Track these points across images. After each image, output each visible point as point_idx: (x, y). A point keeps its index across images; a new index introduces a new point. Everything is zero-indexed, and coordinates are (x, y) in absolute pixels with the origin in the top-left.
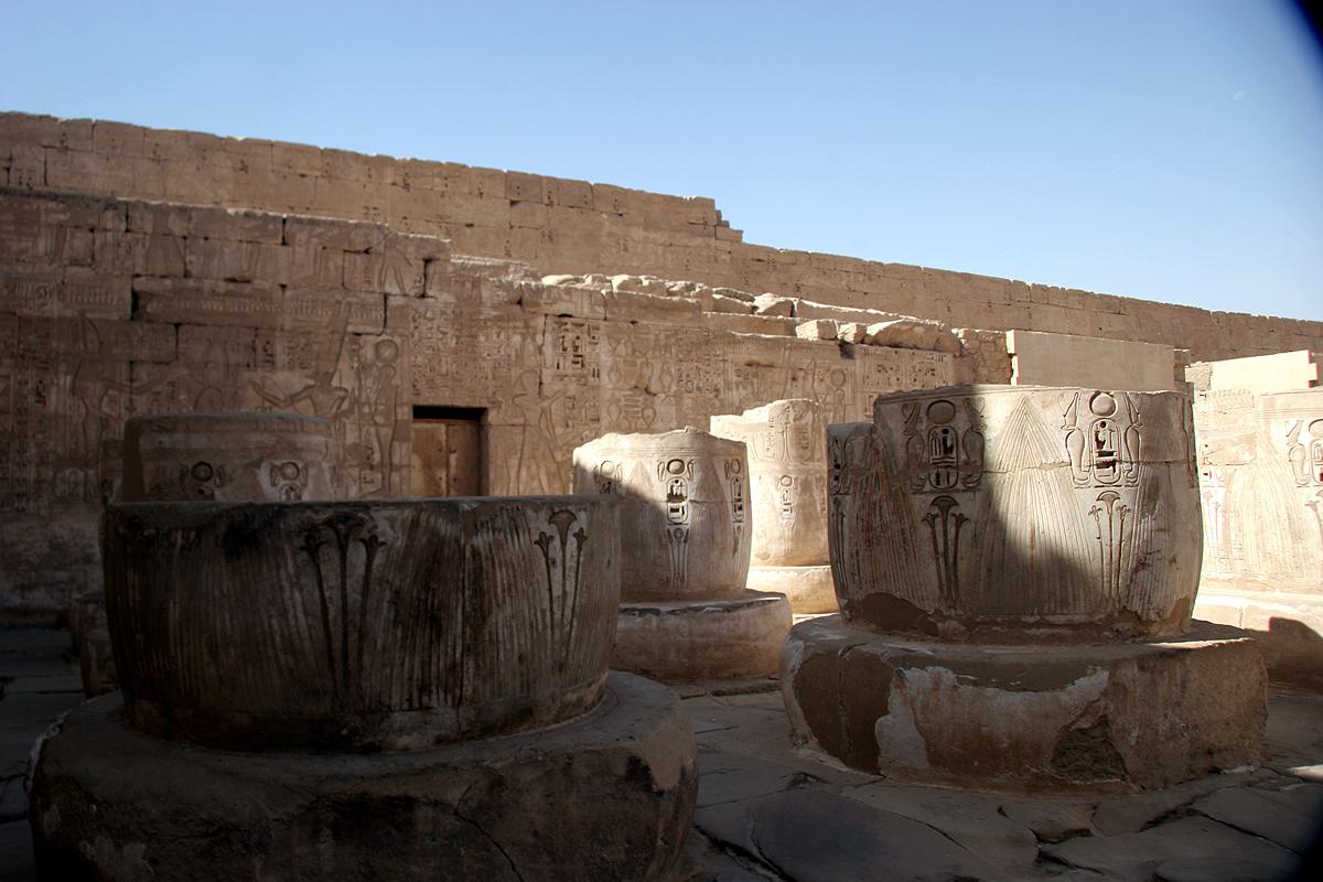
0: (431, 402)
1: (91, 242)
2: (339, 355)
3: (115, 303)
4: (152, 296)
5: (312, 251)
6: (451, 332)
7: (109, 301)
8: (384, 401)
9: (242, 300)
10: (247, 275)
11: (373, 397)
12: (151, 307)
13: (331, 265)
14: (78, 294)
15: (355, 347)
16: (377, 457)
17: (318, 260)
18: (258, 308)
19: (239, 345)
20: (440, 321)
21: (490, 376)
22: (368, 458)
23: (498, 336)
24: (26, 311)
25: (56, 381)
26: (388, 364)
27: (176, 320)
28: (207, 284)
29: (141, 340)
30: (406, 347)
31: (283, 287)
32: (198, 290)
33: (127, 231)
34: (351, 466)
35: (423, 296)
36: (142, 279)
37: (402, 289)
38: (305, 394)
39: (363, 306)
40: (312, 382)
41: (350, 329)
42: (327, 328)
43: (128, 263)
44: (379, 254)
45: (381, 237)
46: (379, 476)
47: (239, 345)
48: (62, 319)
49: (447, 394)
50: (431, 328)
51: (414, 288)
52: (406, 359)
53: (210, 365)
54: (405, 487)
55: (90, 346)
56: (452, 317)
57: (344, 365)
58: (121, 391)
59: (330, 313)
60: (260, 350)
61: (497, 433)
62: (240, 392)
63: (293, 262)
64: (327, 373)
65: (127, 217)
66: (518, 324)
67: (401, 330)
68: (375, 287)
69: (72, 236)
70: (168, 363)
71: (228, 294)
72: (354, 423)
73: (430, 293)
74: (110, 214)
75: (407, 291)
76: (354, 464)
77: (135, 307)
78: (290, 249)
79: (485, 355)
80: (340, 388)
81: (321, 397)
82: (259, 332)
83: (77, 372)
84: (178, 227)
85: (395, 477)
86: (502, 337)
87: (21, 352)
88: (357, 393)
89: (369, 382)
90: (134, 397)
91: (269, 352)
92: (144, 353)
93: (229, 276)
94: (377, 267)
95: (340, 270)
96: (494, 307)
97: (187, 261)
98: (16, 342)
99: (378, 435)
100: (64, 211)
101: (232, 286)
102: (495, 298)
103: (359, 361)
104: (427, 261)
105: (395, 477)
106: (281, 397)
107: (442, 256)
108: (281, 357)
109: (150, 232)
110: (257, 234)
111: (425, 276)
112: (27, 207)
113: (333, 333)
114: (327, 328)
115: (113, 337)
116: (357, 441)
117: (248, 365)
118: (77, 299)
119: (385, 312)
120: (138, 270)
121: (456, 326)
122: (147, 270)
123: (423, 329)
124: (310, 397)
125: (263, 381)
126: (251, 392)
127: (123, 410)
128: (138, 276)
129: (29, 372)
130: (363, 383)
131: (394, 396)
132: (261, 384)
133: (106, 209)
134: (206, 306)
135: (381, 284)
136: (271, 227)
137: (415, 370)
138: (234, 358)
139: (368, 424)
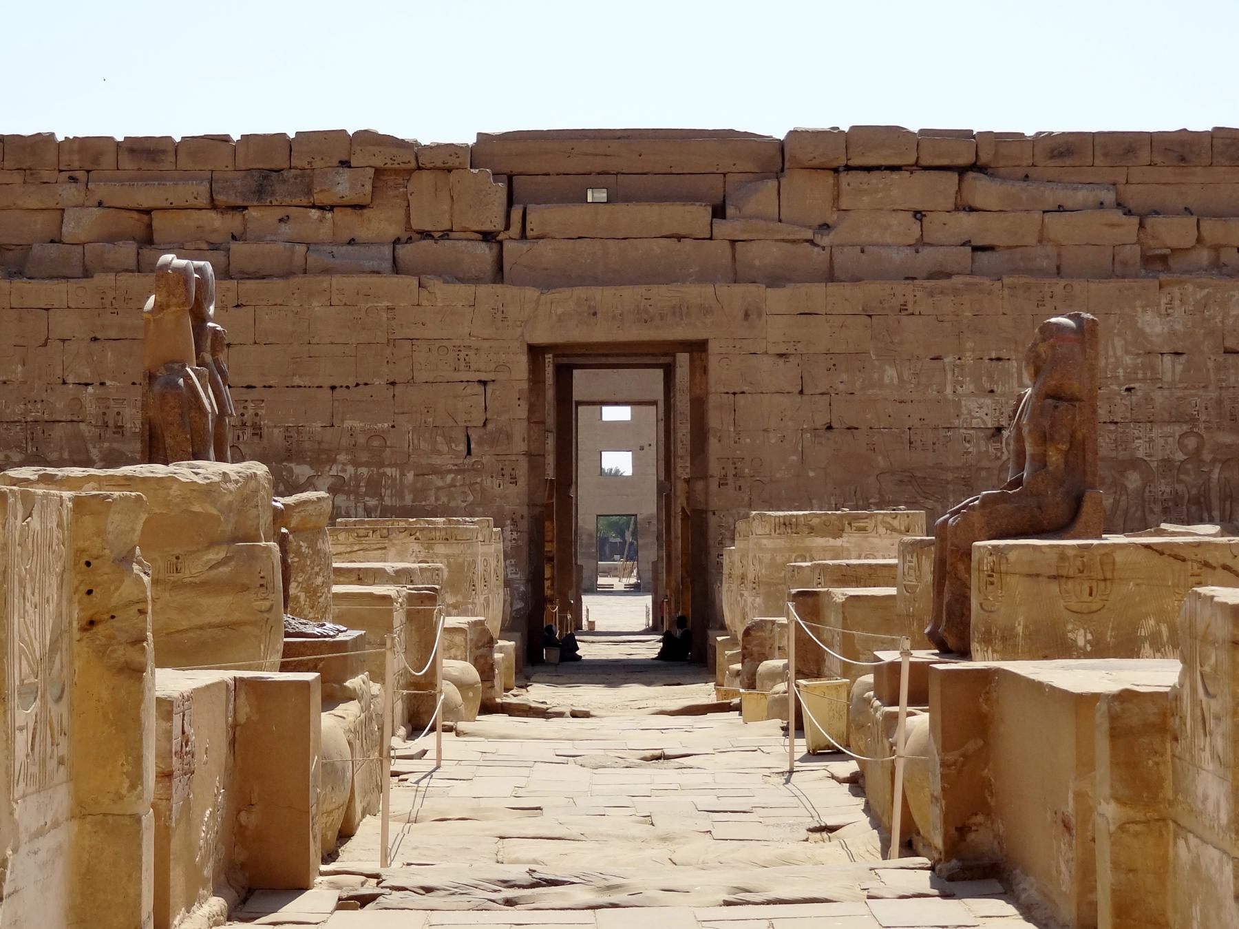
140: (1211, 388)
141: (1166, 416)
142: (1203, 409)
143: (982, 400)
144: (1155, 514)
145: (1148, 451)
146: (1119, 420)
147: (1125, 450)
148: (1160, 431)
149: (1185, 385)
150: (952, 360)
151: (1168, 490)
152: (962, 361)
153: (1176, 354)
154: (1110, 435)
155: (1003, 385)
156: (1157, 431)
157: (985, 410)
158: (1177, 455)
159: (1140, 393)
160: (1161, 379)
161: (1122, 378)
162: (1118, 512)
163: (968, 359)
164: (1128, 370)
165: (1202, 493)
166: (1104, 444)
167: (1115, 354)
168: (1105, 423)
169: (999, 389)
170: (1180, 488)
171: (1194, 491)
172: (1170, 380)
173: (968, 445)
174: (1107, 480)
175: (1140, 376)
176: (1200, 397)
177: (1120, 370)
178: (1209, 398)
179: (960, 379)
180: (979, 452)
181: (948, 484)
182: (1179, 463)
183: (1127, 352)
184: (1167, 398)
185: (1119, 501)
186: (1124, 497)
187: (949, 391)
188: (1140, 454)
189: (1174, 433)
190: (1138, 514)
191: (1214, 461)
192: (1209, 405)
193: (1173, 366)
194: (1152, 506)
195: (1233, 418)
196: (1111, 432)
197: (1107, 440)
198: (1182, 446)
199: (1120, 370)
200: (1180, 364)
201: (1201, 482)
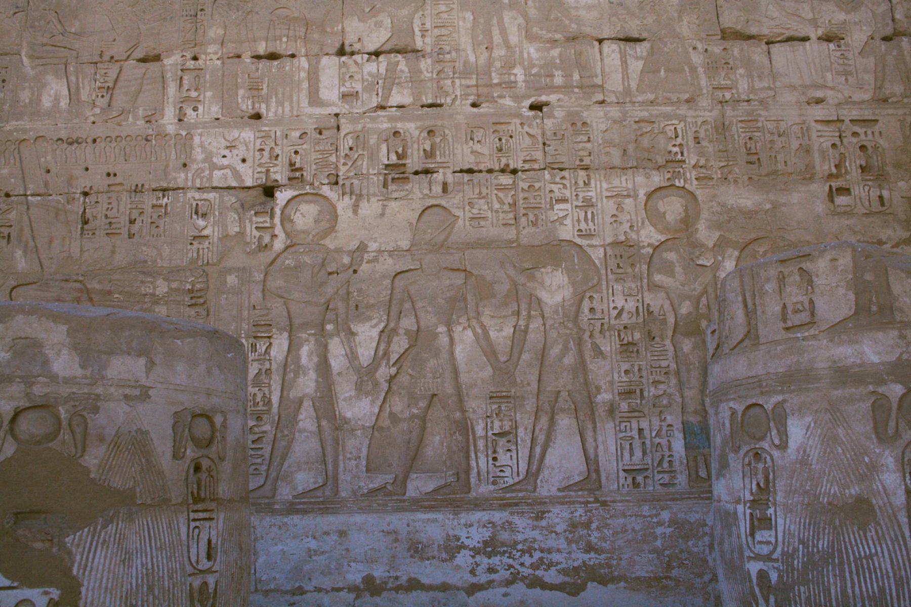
140: (704, 102)
141: (616, 158)
142: (691, 143)
143: (235, 133)
144: (605, 358)
145: (583, 226)
146: (519, 165)
147: (534, 224)
148: (605, 186)
149: (651, 97)
150: (180, 60)
151: (631, 305)
152: (200, 62)
153: (628, 40)
154: (501, 195)
155: (280, 103)
156: (599, 187)
157: (241, 151)
158: (643, 233)
159: (559, 113)
160: (602, 87)
161: (521, 84)
162: (525, 356)
163: (211, 56)
164: (534, 71)
165: (703, 310)
166: (489, 214)
167: (506, 42)
168: (490, 171)
169: (269, 111)
170: (656, 301)
171: (685, 308)
172: (621, 88)
173: (201, 223)
174: (497, 288)
175: (559, 80)
176: (682, 119)
177: (519, 71)
178: (700, 120)
179: (194, 94)
180: (226, 237)
181: (157, 303)
182: (650, 250)
183: (530, 37)
184: (615, 122)
185: (526, 331)
186: (535, 324)
187: (170, 114)
188: (566, 232)
189: (635, 190)
190: (569, 360)
191: (721, 245)
192: (702, 134)
193: (624, 63)
194: (599, 340)
195: (754, 158)
196: (501, 188)
197: (496, 206)
198: (655, 217)
199: (519, 71)
200: (637, 58)
201: (699, 289)
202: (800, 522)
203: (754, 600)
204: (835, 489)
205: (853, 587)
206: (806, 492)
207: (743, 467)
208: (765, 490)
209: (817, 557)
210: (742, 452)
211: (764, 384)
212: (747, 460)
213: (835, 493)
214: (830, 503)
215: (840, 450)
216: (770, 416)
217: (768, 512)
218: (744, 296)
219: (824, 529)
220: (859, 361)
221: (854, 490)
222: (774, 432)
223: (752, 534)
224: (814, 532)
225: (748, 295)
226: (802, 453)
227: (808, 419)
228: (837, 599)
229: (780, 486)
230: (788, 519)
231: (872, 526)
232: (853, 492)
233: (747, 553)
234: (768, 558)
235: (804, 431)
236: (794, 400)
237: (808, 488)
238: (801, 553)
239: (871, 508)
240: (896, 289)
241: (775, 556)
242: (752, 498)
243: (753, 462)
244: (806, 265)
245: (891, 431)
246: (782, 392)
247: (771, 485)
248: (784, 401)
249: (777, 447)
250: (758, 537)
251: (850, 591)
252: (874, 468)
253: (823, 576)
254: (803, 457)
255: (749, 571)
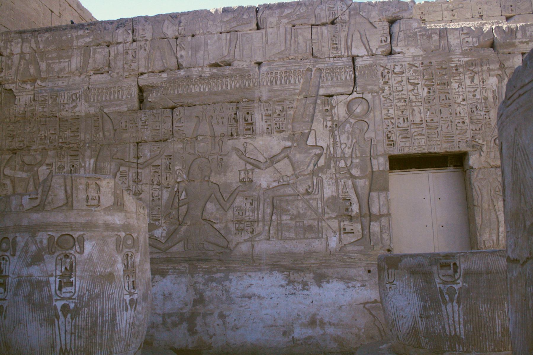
0: (406, 151)
1: (107, 55)
2: (313, 115)
3: (124, 97)
4: (152, 87)
5: (282, 30)
6: (421, 82)
7: (120, 97)
8: (359, 155)
9: (224, 80)
10: (227, 59)
11: (348, 151)
12: (151, 97)
13: (300, 39)
14: (98, 96)
15: (328, 108)
16: (355, 208)
17: (288, 37)
18: (238, 85)
19: (223, 118)
20: (410, 73)
21: (467, 121)
22: (347, 209)
23: (472, 81)
24: (64, 113)
25: (83, 165)
26: (361, 120)
27: (171, 104)
28: (195, 72)
29: (145, 124)
30: (377, 101)
31: (259, 64)
32: (188, 77)
33: (134, 41)
34: (331, 218)
35: (391, 53)
36: (146, 76)
37: (369, 50)
38: (283, 155)
39: (332, 70)
40: (289, 144)
41: (322, 92)
42: (299, 94)
43: (134, 66)
44: (344, 22)
45: (346, 8)
46: (359, 227)
47: (223, 118)
48: (88, 116)
49: (423, 142)
50: (402, 81)
51: (380, 47)
52: (378, 113)
53: (199, 139)
54: (385, 236)
55: (107, 134)
56: (422, 68)
57: (318, 126)
58: (130, 167)
59: (302, 81)
60: (241, 121)
61: (480, 176)
62: (225, 158)
63: (267, 42)
64: (302, 134)
65: (133, 32)
66: (492, 67)
67: (370, 87)
68: (343, 51)
69: (95, 53)
70: (166, 140)
71: (212, 77)
72: (332, 178)
73: (396, 49)
74: (120, 31)
75: (374, 52)
76: (334, 215)
77: (141, 101)
78: (263, 31)
79: (459, 100)
80: (316, 146)
81: (298, 156)
82: (239, 105)
83: (97, 158)
84: (170, 31)
85: (375, 227)
86: (476, 81)
87: (60, 145)
88: (332, 149)
89: (344, 138)
90: (139, 171)
91: (250, 121)
92: (147, 134)
93: (213, 62)
94: (343, 35)
95: (309, 42)
96: (464, 53)
97: (178, 56)
98: (57, 137)
99: (355, 187)
100: (88, 36)
101: (215, 70)
102: (465, 45)
103: (332, 120)
104: (392, 22)
105: (375, 227)
106: (262, 159)
107: (405, 15)
108: (260, 124)
109: (149, 39)
110: (234, 24)
111: (391, 36)
112: (64, 38)
113: (306, 97)
114: (299, 94)
115: (123, 125)
116: (334, 194)
117: (232, 135)
118: (98, 100)
119: (355, 74)
120: (142, 70)
121: (426, 77)
122: (148, 68)
123: (393, 83)
124: (288, 157)
125: (245, 148)
126: (234, 157)
127: (131, 183)
128: (142, 74)
129: (65, 159)
130: (338, 139)
131: (368, 149)
132: (243, 150)
133: (118, 27)
134: (195, 89)
135: (348, 48)
136: (245, 17)
137: (388, 122)
138: (219, 130)
139: (347, 178)
202: (87, 283)
203: (56, 317)
204: (102, 270)
205: (106, 306)
206: (91, 271)
207: (56, 260)
208: (70, 270)
209: (94, 296)
210: (56, 255)
211: (74, 226)
212: (59, 258)
213: (102, 271)
214: (100, 275)
215: (105, 255)
216: (76, 240)
217: (71, 279)
218: (65, 186)
219: (98, 285)
220: (113, 222)
221: (109, 270)
222: (77, 247)
223: (60, 289)
224: (93, 286)
225: (69, 189)
226: (90, 255)
227: (94, 242)
228: (100, 312)
229: (79, 269)
230: (82, 282)
231: (113, 283)
232: (108, 271)
233: (55, 298)
234: (70, 298)
235: (92, 247)
236: (88, 234)
237: (91, 269)
238: (87, 295)
239: (114, 275)
240: (125, 199)
241: (74, 297)
242: (61, 274)
243: (63, 258)
244: (98, 182)
245: (120, 249)
246: (83, 231)
247: (74, 268)
248: (84, 234)
249: (78, 253)
250: (64, 290)
251: (105, 307)
252: (115, 261)
253: (96, 303)
254: (90, 257)
255: (55, 306)
